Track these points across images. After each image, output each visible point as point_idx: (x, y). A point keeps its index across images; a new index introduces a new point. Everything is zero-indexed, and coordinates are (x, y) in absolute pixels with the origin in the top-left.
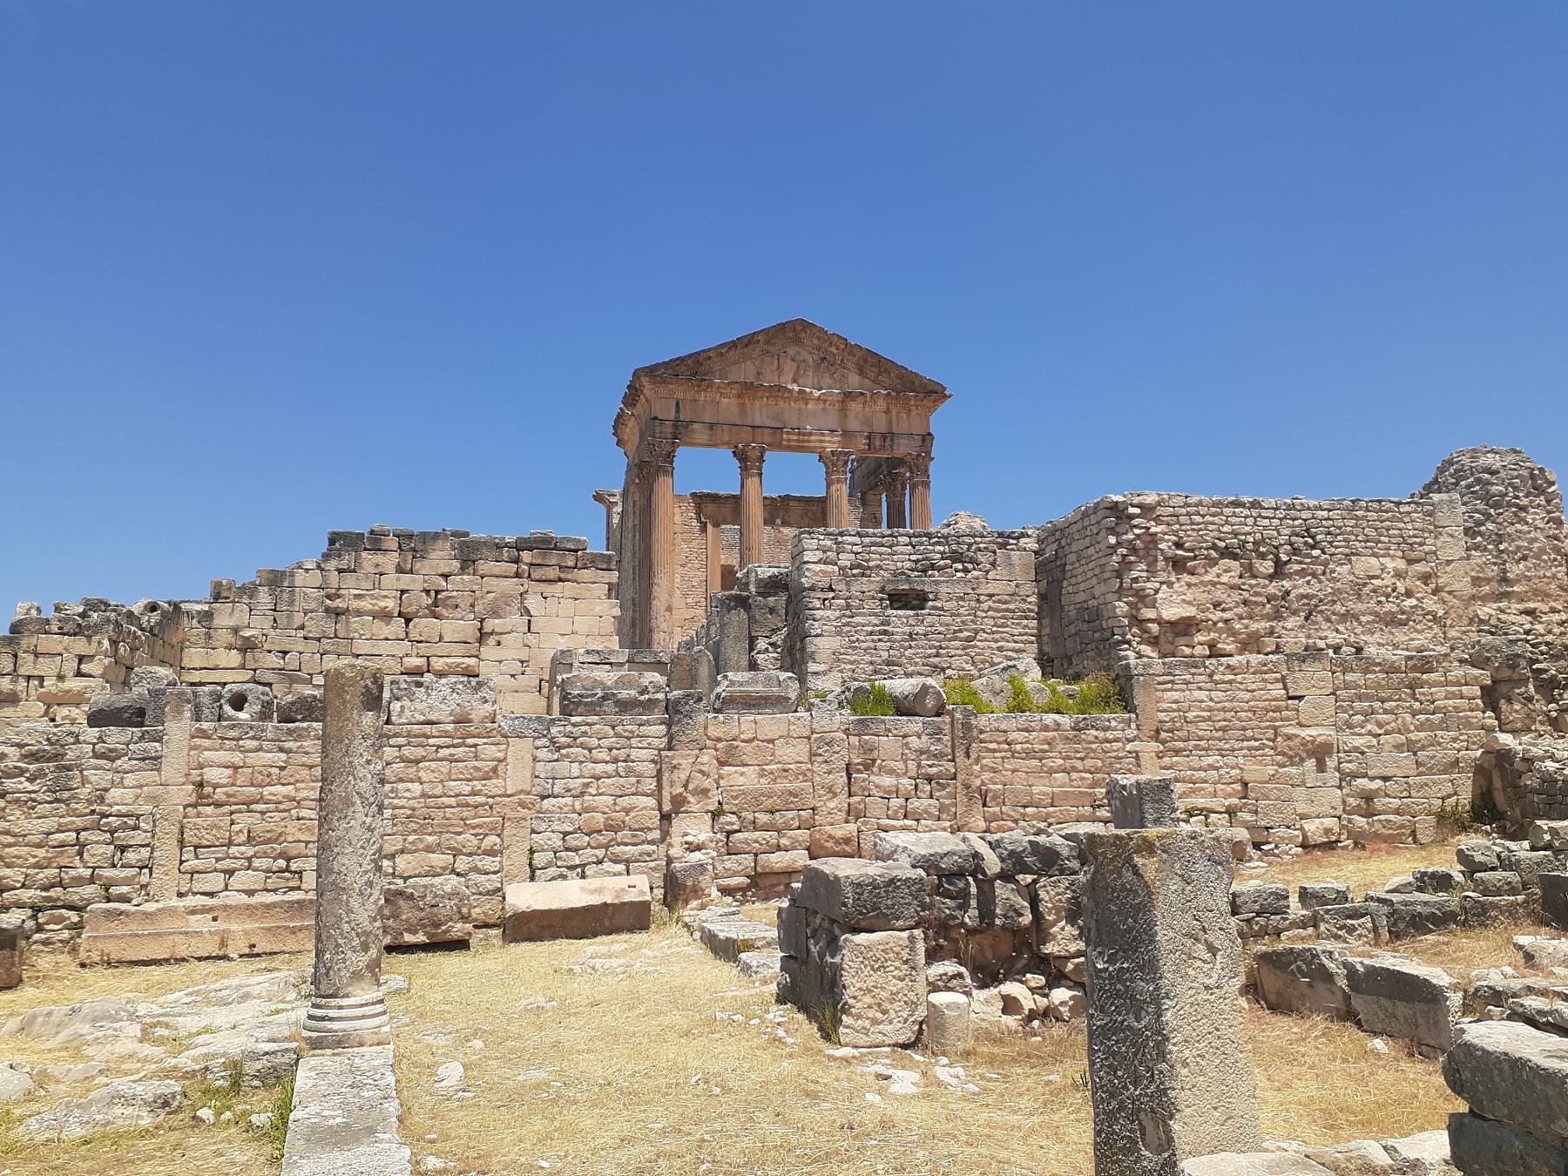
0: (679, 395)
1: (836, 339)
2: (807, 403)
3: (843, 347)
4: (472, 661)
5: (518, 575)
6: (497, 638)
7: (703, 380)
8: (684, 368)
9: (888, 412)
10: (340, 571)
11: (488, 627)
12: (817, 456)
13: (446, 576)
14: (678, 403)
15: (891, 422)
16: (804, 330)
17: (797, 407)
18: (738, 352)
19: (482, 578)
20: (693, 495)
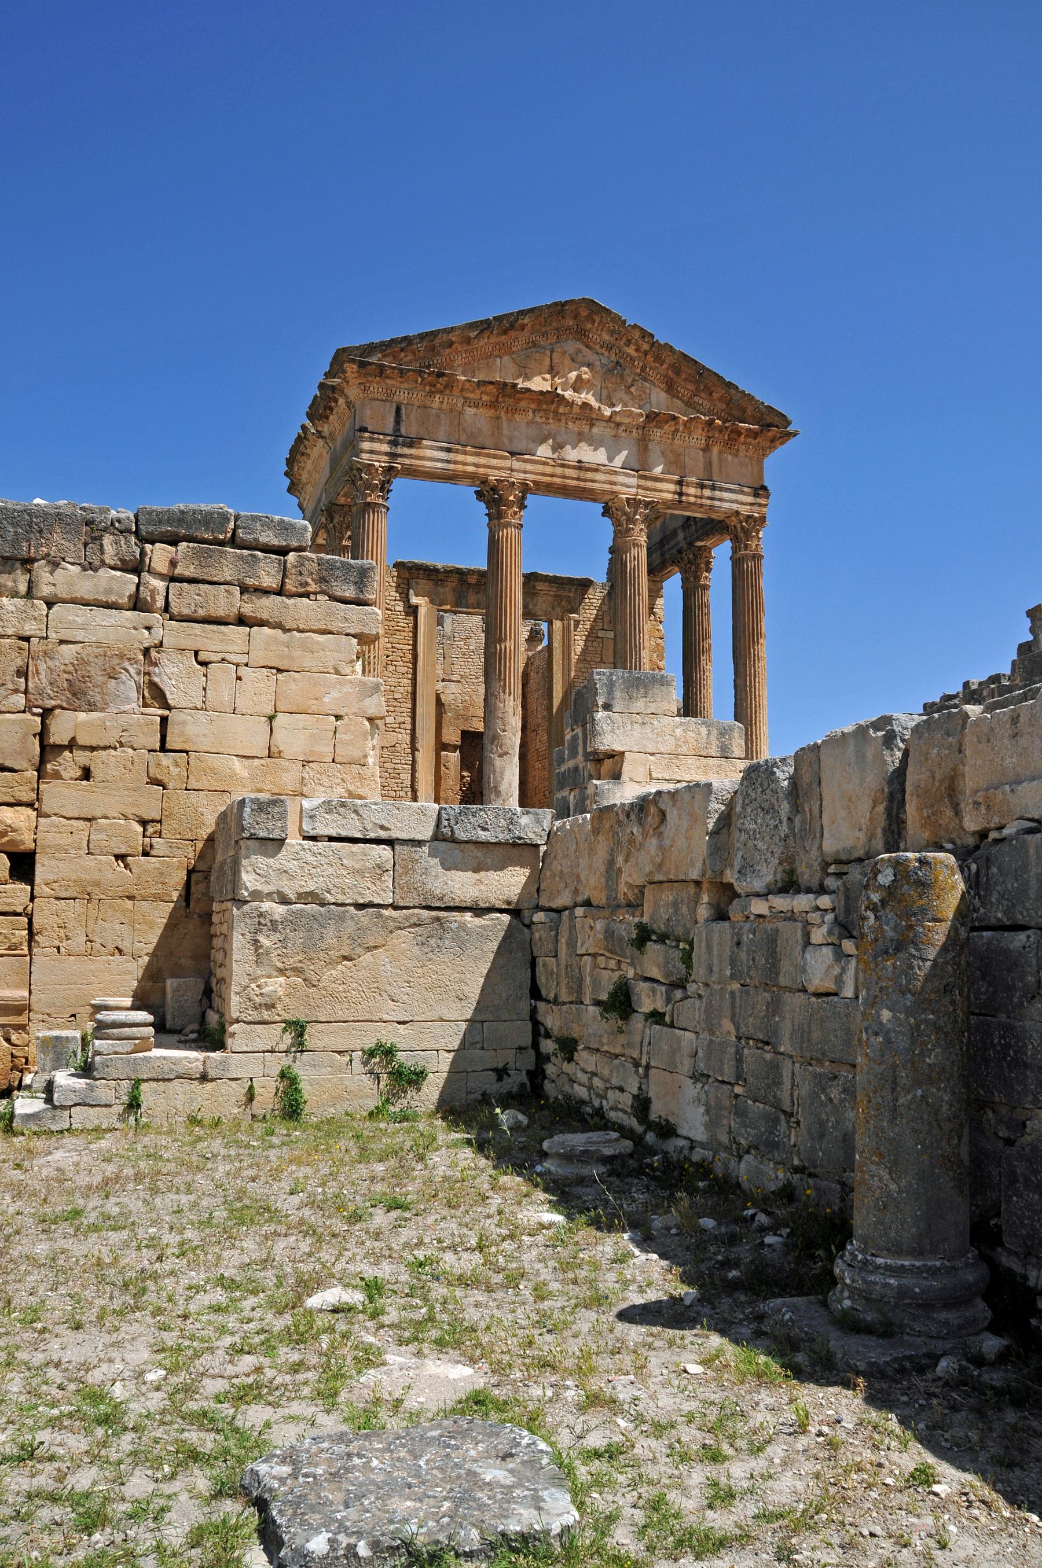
0: (402, 397)
1: (637, 334)
2: (592, 425)
3: (646, 347)
5: (137, 604)
6: (82, 757)
7: (440, 375)
8: (410, 357)
9: (706, 449)
11: (59, 735)
12: (599, 508)
14: (398, 410)
15: (710, 463)
16: (590, 318)
17: (576, 429)
18: (493, 340)
19: (50, 604)
20: (397, 565)
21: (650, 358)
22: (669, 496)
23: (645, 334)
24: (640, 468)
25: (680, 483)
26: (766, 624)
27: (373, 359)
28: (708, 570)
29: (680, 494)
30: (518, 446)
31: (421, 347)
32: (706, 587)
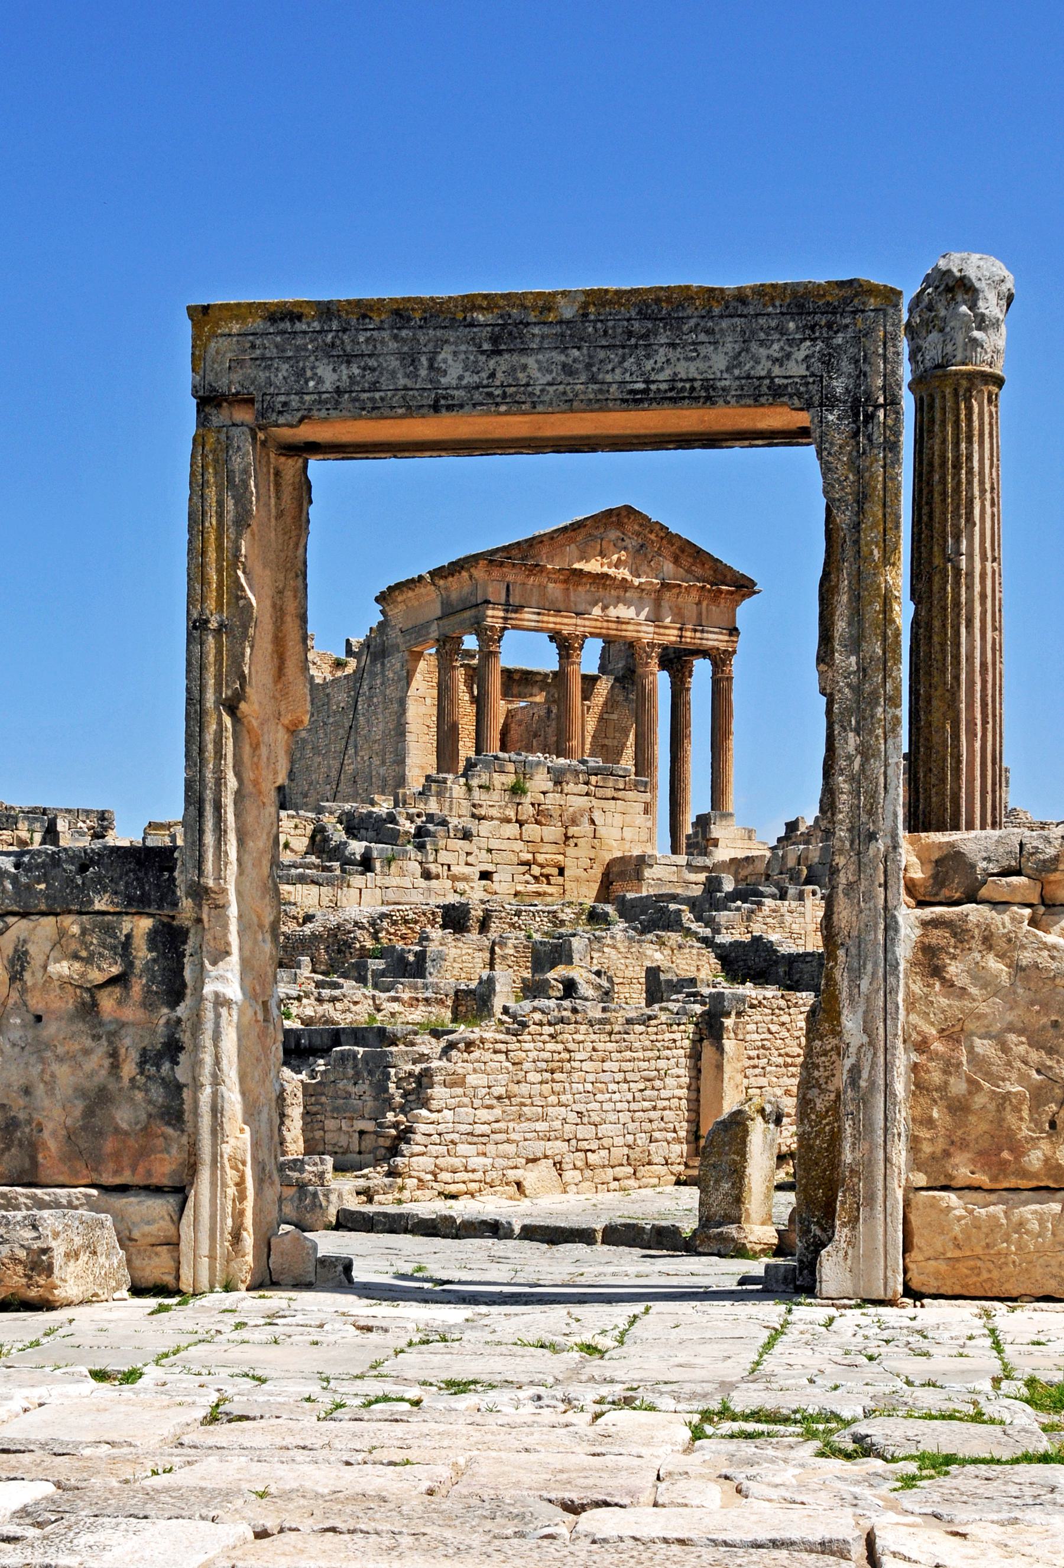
0: (510, 578)
1: (658, 527)
4: (561, 857)
5: (587, 794)
9: (699, 603)
10: (480, 787)
13: (544, 793)
21: (665, 542)
22: (673, 639)
23: (663, 528)
24: (655, 619)
25: (681, 629)
26: (735, 726)
27: (497, 557)
28: (690, 676)
29: (681, 637)
30: (581, 608)
31: (525, 546)
32: (688, 689)
